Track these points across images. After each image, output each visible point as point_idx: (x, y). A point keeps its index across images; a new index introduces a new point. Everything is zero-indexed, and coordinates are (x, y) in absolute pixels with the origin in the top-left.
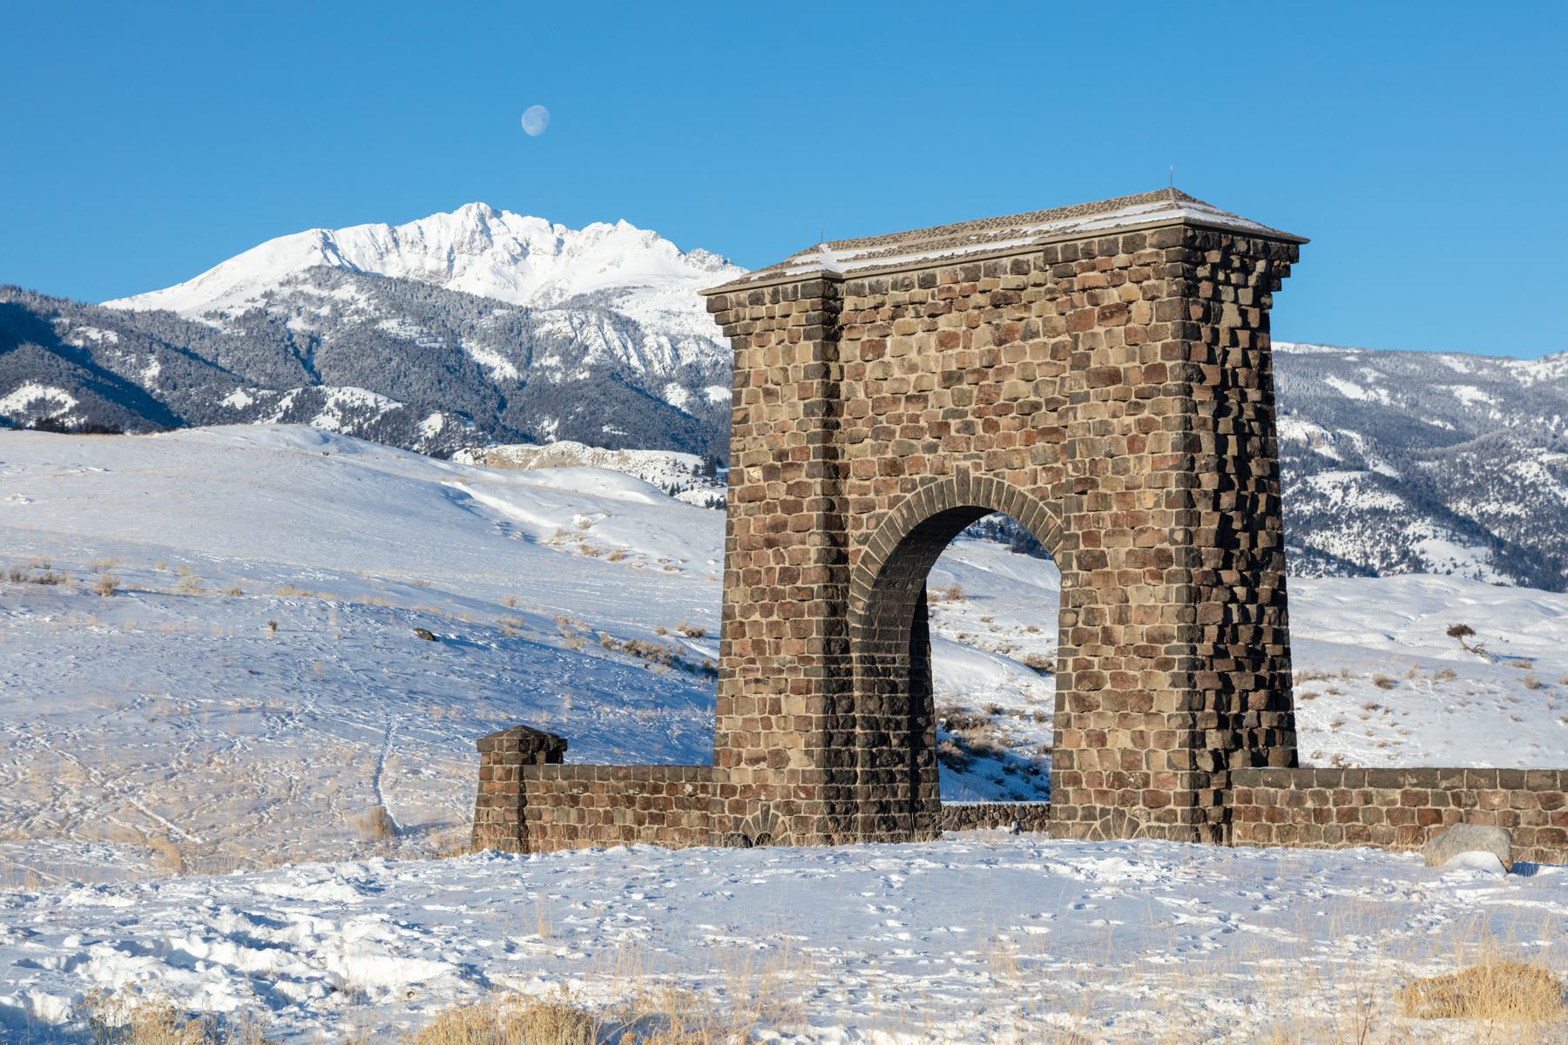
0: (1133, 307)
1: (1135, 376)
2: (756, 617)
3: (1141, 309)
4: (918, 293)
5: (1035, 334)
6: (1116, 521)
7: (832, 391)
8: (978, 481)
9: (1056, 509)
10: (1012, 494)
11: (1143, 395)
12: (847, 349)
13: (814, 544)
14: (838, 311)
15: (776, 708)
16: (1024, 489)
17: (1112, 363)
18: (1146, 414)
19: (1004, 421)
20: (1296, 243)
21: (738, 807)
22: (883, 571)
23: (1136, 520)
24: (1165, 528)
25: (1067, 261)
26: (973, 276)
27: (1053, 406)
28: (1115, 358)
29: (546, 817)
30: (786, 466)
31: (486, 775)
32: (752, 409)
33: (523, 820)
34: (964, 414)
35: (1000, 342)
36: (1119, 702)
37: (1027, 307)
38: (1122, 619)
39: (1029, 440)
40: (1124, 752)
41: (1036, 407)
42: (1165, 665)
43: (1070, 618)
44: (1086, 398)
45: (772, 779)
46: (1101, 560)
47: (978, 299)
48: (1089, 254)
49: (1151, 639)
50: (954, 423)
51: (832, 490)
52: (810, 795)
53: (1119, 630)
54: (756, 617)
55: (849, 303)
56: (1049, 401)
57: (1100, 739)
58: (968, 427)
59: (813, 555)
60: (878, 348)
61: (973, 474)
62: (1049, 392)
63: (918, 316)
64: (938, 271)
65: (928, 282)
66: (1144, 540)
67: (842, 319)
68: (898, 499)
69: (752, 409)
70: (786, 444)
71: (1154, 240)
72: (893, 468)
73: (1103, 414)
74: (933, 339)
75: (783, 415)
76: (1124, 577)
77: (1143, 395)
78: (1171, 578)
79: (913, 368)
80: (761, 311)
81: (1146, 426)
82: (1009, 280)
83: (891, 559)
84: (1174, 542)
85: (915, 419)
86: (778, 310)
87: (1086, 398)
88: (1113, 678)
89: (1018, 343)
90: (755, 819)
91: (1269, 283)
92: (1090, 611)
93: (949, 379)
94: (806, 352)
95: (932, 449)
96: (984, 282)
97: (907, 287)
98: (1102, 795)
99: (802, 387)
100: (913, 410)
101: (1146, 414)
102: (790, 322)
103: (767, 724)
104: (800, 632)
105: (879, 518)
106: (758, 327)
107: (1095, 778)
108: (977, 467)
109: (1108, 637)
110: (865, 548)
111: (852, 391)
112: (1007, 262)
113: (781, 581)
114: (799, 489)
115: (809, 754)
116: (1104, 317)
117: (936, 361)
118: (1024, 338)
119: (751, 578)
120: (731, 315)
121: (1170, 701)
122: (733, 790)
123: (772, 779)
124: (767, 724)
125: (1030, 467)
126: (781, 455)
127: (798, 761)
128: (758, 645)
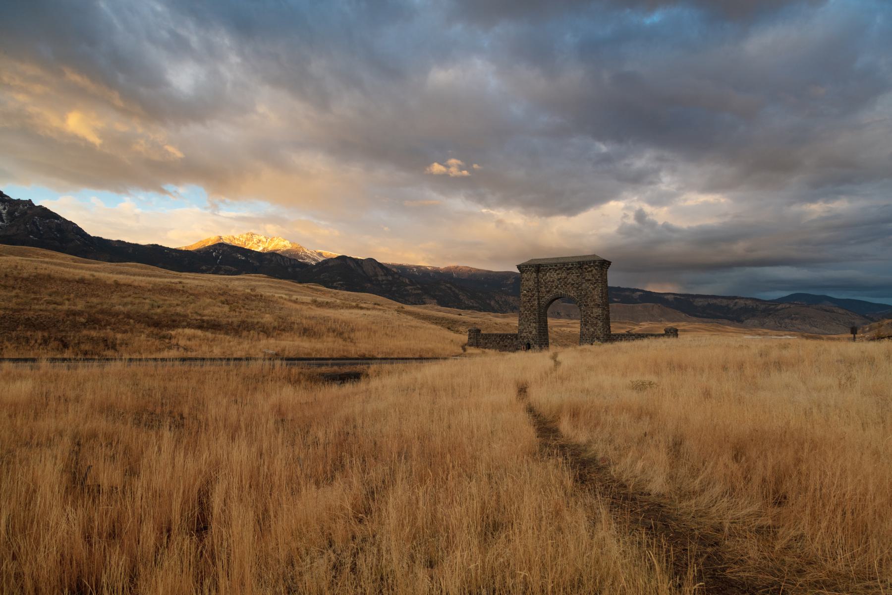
4: (554, 267)
7: (538, 280)
11: (595, 283)
12: (541, 275)
13: (536, 302)
15: (530, 325)
16: (572, 295)
21: (523, 339)
23: (594, 300)
24: (599, 301)
26: (564, 265)
27: (577, 284)
36: (591, 324)
45: (529, 335)
57: (588, 329)
65: (556, 266)
70: (531, 287)
72: (548, 292)
73: (588, 285)
76: (592, 308)
77: (595, 283)
81: (596, 287)
82: (570, 266)
93: (558, 280)
94: (534, 275)
96: (566, 266)
104: (535, 315)
109: (590, 316)
114: (534, 295)
116: (588, 272)
123: (529, 335)
128: (527, 316)
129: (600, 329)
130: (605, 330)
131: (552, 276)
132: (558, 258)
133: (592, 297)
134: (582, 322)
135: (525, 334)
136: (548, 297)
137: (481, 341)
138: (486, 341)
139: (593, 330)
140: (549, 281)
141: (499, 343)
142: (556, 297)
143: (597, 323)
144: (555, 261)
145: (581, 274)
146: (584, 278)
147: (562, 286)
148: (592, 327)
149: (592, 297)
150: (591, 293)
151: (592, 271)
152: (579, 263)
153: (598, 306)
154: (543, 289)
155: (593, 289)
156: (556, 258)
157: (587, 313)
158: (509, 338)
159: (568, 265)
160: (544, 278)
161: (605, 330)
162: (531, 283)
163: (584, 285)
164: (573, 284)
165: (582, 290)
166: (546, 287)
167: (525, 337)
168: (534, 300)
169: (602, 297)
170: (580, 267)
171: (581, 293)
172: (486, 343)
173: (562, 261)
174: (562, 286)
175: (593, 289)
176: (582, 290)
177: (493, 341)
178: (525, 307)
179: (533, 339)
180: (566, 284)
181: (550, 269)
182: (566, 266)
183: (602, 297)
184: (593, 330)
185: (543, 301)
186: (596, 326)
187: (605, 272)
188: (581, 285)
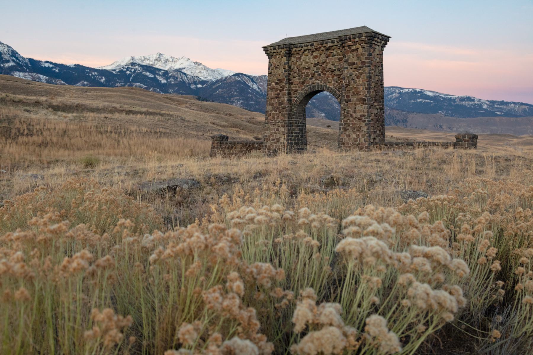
0: (359, 50)
1: (358, 63)
2: (273, 112)
3: (361, 50)
4: (309, 47)
5: (335, 55)
6: (354, 93)
7: (290, 67)
8: (321, 85)
9: (339, 91)
10: (329, 88)
12: (293, 59)
13: (286, 98)
15: (277, 130)
16: (332, 87)
17: (353, 61)
18: (361, 71)
19: (327, 73)
20: (389, 37)
22: (300, 103)
24: (364, 94)
25: (345, 40)
27: (339, 70)
28: (354, 60)
31: (213, 143)
32: (273, 71)
35: (327, 57)
36: (354, 129)
37: (334, 49)
38: (355, 112)
40: (354, 138)
41: (335, 70)
42: (364, 121)
43: (343, 112)
44: (347, 68)
46: (350, 100)
47: (323, 48)
48: (350, 39)
49: (361, 116)
51: (289, 87)
54: (273, 112)
55: (294, 49)
57: (349, 136)
58: (319, 75)
59: (286, 99)
60: (300, 59)
62: (338, 67)
64: (314, 43)
65: (312, 45)
66: (360, 96)
67: (292, 53)
69: (273, 71)
70: (280, 78)
71: (365, 35)
72: (303, 83)
73: (351, 71)
74: (312, 57)
75: (280, 72)
77: (361, 68)
78: (366, 104)
79: (307, 63)
80: (275, 51)
81: (361, 74)
82: (330, 44)
83: (301, 101)
84: (366, 97)
85: (308, 73)
86: (279, 51)
87: (347, 68)
88: (352, 124)
91: (383, 46)
92: (348, 111)
93: (315, 65)
94: (285, 59)
95: (311, 79)
96: (324, 45)
97: (307, 46)
99: (284, 66)
100: (307, 71)
101: (361, 71)
102: (281, 54)
103: (275, 133)
104: (283, 115)
105: (299, 93)
106: (274, 54)
108: (321, 82)
109: (351, 116)
113: (279, 105)
114: (283, 87)
116: (352, 51)
117: (313, 61)
118: (332, 56)
120: (269, 52)
121: (365, 128)
124: (275, 133)
125: (333, 82)
126: (279, 80)
128: (274, 118)
129: (363, 136)
131: (308, 60)
132: (316, 35)
134: (341, 125)
136: (302, 91)
140: (303, 68)
143: (360, 127)
144: (311, 40)
147: (319, 75)
148: (354, 132)
153: (363, 101)
156: (314, 35)
159: (327, 43)
160: (298, 63)
162: (281, 71)
163: (345, 72)
164: (333, 71)
165: (344, 79)
166: (301, 77)
173: (320, 38)
176: (344, 79)
178: (272, 104)
180: (324, 72)
181: (305, 50)
182: (324, 45)
183: (369, 88)
184: (354, 136)
185: (297, 97)
186: (359, 131)
187: (377, 52)
188: (342, 71)
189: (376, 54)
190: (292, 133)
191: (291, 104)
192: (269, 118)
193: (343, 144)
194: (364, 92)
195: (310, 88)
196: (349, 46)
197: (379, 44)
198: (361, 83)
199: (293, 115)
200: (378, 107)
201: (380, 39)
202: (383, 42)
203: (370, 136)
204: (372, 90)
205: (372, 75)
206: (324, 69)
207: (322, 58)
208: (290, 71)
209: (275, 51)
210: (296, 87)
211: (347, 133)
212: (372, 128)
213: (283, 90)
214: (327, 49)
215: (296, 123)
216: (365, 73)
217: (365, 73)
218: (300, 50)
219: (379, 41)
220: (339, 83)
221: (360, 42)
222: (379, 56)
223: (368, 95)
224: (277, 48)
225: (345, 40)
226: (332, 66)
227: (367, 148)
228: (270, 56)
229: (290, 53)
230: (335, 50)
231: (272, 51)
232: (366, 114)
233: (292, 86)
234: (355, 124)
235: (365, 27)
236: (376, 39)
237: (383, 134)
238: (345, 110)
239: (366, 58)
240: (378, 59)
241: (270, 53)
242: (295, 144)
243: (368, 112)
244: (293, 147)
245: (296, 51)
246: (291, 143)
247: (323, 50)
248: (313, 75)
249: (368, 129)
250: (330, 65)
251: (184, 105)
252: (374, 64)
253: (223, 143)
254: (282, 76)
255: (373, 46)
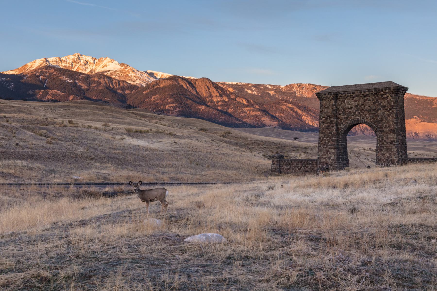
2: (325, 138)
4: (351, 94)
5: (371, 100)
6: (386, 126)
7: (337, 107)
8: (361, 120)
9: (374, 124)
10: (367, 122)
12: (339, 102)
14: (337, 96)
15: (329, 151)
16: (369, 121)
17: (385, 105)
18: (390, 112)
19: (365, 112)
21: (322, 165)
22: (344, 132)
24: (393, 127)
26: (361, 93)
27: (374, 110)
28: (385, 104)
29: (284, 167)
30: (330, 118)
31: (273, 161)
33: (280, 167)
34: (358, 111)
35: (365, 101)
36: (387, 150)
37: (369, 96)
39: (369, 115)
41: (371, 110)
42: (394, 145)
43: (379, 139)
44: (381, 109)
45: (328, 161)
47: (361, 95)
48: (382, 90)
50: (357, 112)
51: (337, 121)
52: (335, 162)
53: (387, 140)
54: (325, 138)
55: (340, 95)
56: (373, 110)
57: (384, 154)
59: (335, 130)
60: (344, 102)
61: (360, 119)
63: (351, 97)
66: (391, 128)
68: (347, 122)
70: (329, 115)
71: (393, 88)
72: (347, 118)
73: (383, 111)
76: (387, 133)
77: (390, 109)
79: (350, 104)
80: (326, 96)
81: (391, 113)
82: (367, 93)
83: (346, 130)
85: (350, 111)
86: (328, 96)
87: (381, 109)
89: (367, 101)
90: (325, 166)
92: (382, 138)
93: (356, 106)
94: (333, 102)
95: (353, 115)
96: (363, 93)
97: (349, 93)
98: (384, 162)
101: (390, 112)
102: (330, 98)
103: (327, 153)
104: (333, 141)
105: (344, 125)
107: (383, 160)
108: (361, 118)
109: (385, 141)
110: (341, 129)
111: (339, 107)
112: (367, 91)
114: (332, 122)
115: (335, 157)
116: (384, 98)
118: (369, 101)
119: (324, 133)
120: (320, 97)
121: (395, 149)
122: (321, 162)
124: (327, 153)
127: (333, 158)
128: (325, 142)
129: (394, 154)
130: (401, 154)
131: (350, 103)
132: (355, 86)
133: (387, 123)
135: (324, 160)
136: (346, 124)
137: (284, 166)
138: (289, 167)
139: (388, 155)
140: (347, 108)
141: (300, 169)
142: (354, 123)
143: (392, 148)
144: (353, 89)
145: (377, 100)
146: (380, 105)
147: (359, 113)
148: (387, 152)
149: (387, 123)
150: (387, 119)
151: (387, 97)
152: (375, 89)
154: (341, 116)
155: (388, 116)
156: (353, 85)
157: (382, 139)
158: (310, 164)
159: (364, 92)
160: (342, 105)
161: (401, 154)
162: (330, 110)
165: (378, 116)
166: (344, 114)
167: (324, 162)
168: (333, 127)
169: (397, 123)
170: (376, 94)
171: (377, 119)
172: (289, 169)
173: (359, 88)
174: (359, 113)
175: (388, 116)
177: (295, 167)
179: (332, 165)
181: (348, 96)
182: (363, 93)
183: (397, 123)
184: (388, 155)
185: (342, 128)
187: (400, 98)
188: (377, 111)
189: (400, 100)
190: (339, 153)
191: (338, 133)
192: (321, 143)
193: (380, 160)
194: (394, 125)
195: (352, 121)
196: (381, 95)
197: (402, 93)
198: (391, 119)
199: (340, 140)
200: (402, 135)
201: (402, 90)
202: (404, 92)
203: (398, 155)
204: (399, 124)
205: (398, 114)
206: (363, 109)
207: (361, 102)
208: (337, 110)
209: (326, 96)
210: (342, 121)
211: (382, 153)
212: (400, 149)
213: (332, 123)
214: (365, 96)
215: (342, 146)
216: (394, 113)
217: (394, 113)
218: (344, 96)
219: (402, 91)
220: (374, 119)
221: (389, 93)
222: (402, 101)
223: (396, 128)
224: (327, 94)
225: (378, 91)
226: (369, 108)
227: (397, 162)
228: (321, 99)
229: (337, 98)
230: (370, 97)
231: (323, 96)
232: (395, 140)
233: (338, 120)
234: (388, 146)
235: (391, 82)
236: (400, 91)
237: (406, 153)
238: (380, 137)
239: (394, 103)
240: (401, 103)
241: (321, 97)
242: (342, 160)
243: (397, 138)
244: (340, 162)
245: (341, 96)
246: (339, 160)
247: (362, 97)
248: (354, 113)
249: (397, 150)
250: (367, 107)
251: (154, 121)
252: (399, 107)
253: (282, 161)
254: (331, 114)
255: (398, 95)
